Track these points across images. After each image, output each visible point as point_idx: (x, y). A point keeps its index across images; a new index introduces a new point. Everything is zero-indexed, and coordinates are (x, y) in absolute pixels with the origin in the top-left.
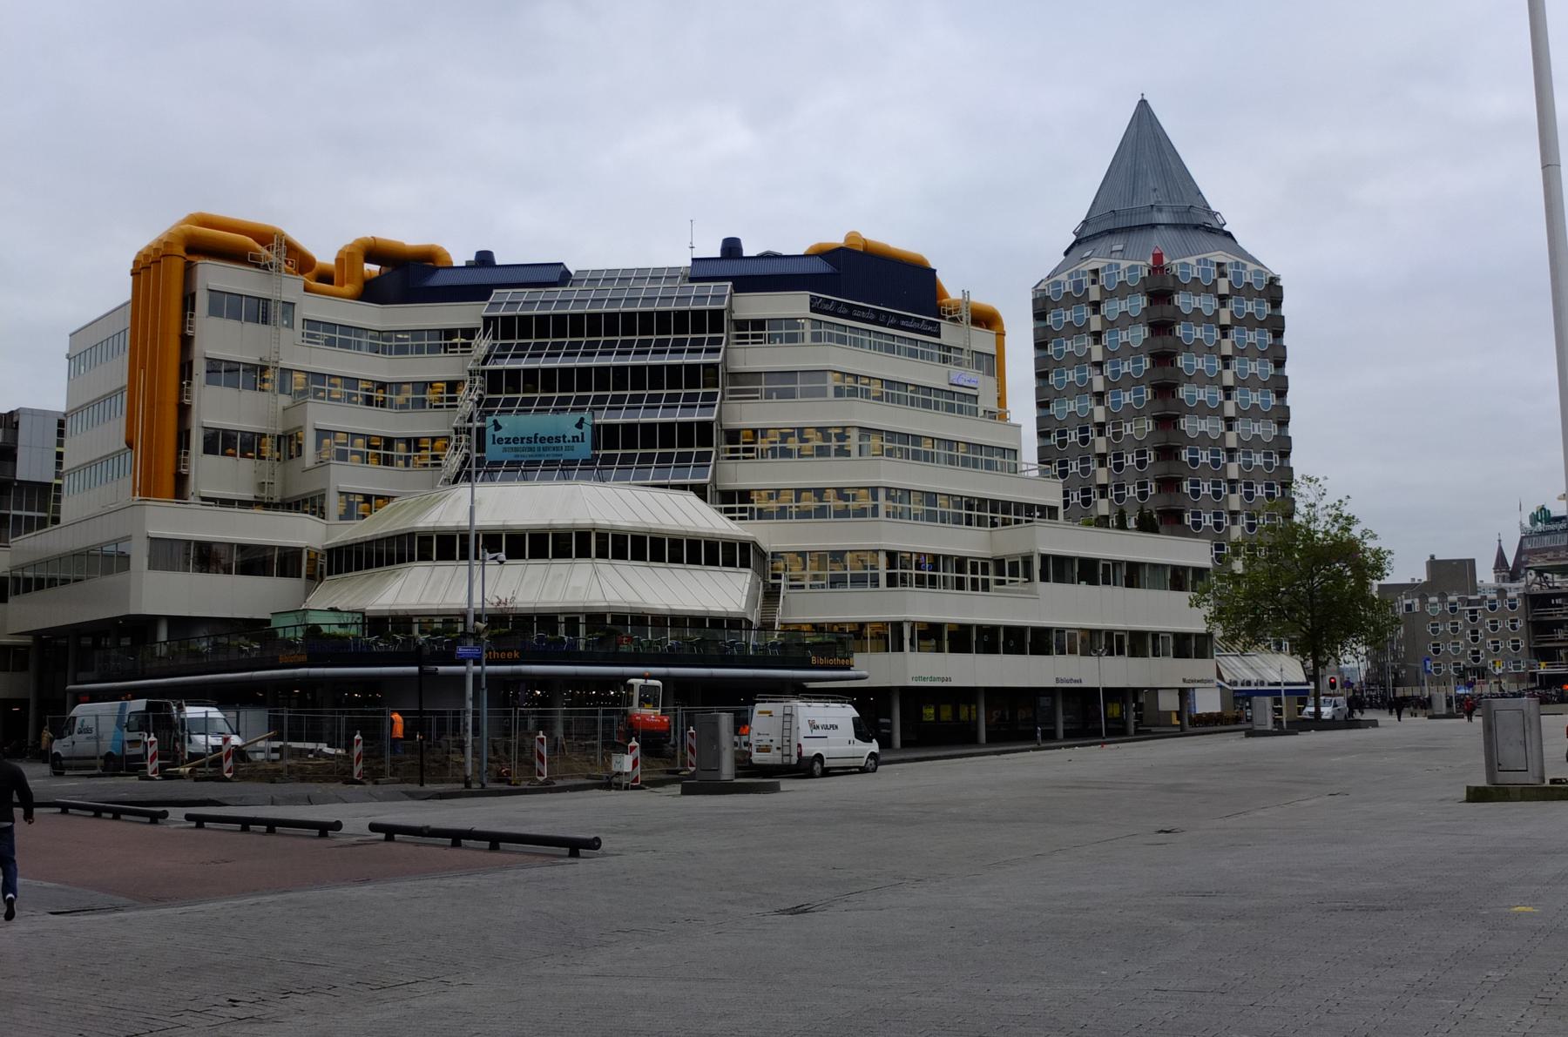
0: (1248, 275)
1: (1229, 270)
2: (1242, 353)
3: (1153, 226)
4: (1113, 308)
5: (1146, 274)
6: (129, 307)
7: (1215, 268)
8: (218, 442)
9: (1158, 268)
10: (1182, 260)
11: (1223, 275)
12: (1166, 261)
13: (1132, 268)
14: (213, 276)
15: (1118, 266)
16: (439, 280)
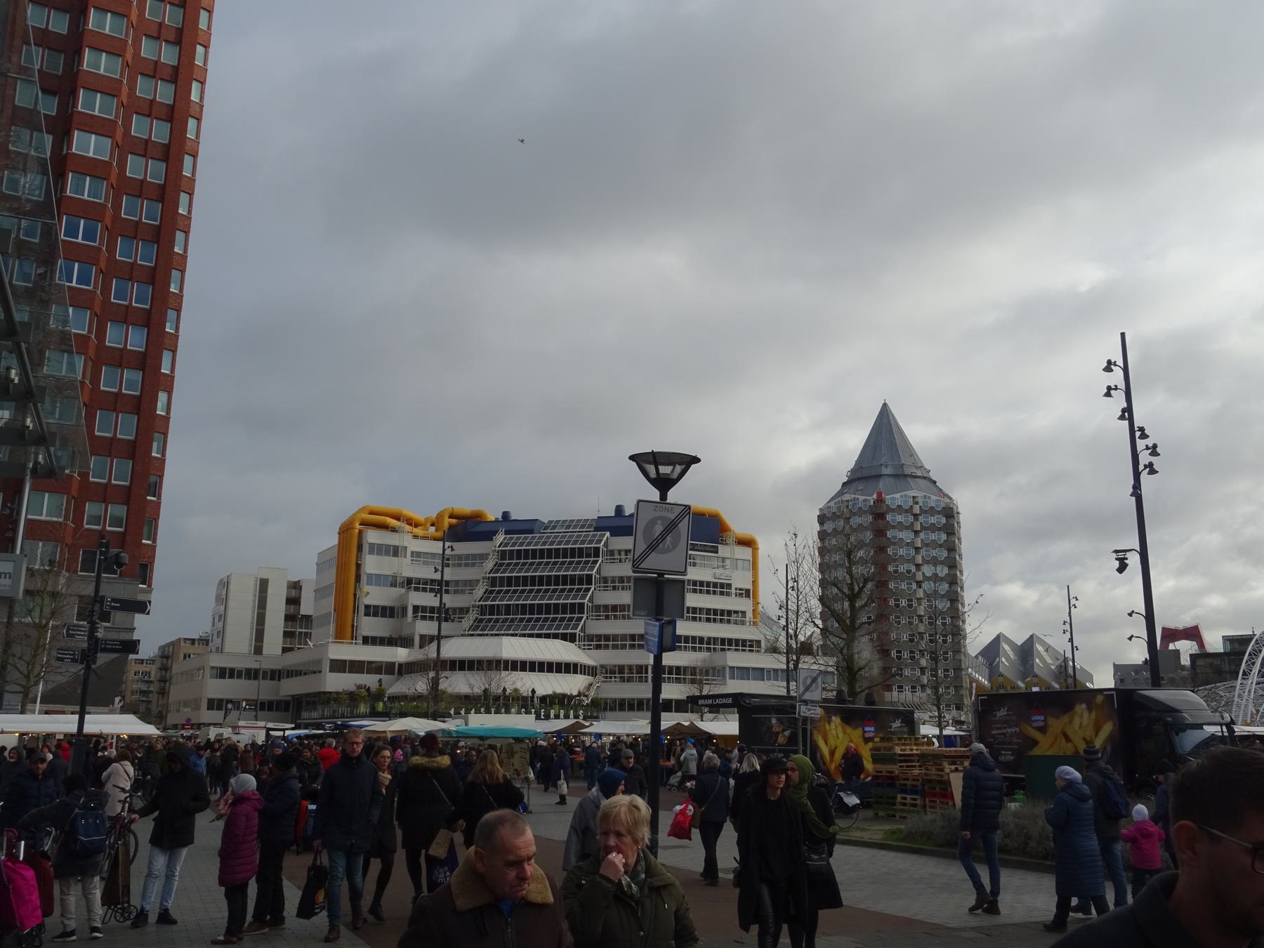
0: (932, 503)
1: (920, 500)
2: (927, 545)
3: (881, 476)
4: (856, 521)
5: (872, 504)
6: (337, 547)
7: (912, 499)
8: (372, 611)
9: (880, 500)
10: (891, 496)
11: (917, 503)
12: (883, 495)
13: (865, 501)
14: (373, 536)
15: (858, 499)
16: (480, 528)
